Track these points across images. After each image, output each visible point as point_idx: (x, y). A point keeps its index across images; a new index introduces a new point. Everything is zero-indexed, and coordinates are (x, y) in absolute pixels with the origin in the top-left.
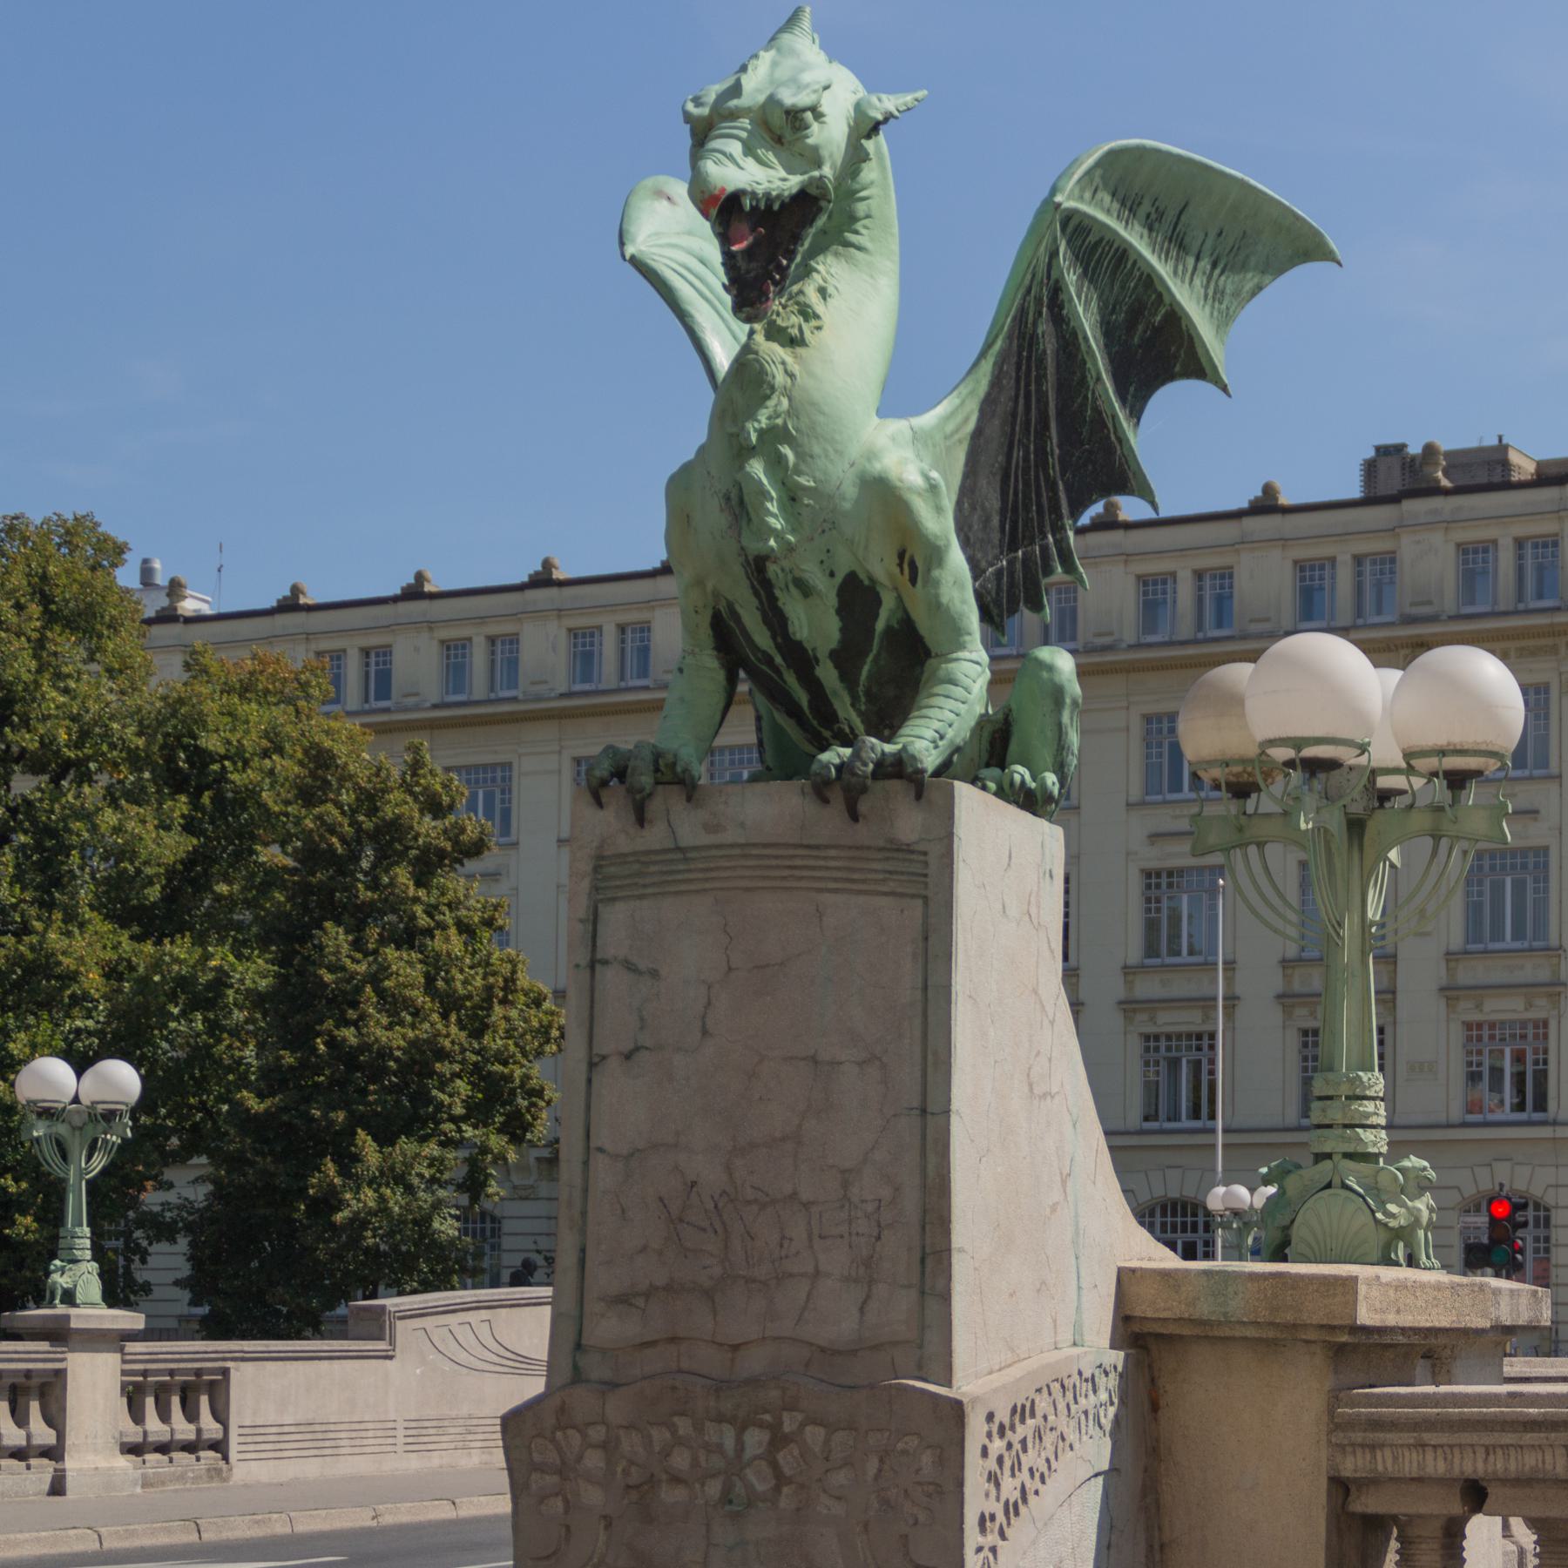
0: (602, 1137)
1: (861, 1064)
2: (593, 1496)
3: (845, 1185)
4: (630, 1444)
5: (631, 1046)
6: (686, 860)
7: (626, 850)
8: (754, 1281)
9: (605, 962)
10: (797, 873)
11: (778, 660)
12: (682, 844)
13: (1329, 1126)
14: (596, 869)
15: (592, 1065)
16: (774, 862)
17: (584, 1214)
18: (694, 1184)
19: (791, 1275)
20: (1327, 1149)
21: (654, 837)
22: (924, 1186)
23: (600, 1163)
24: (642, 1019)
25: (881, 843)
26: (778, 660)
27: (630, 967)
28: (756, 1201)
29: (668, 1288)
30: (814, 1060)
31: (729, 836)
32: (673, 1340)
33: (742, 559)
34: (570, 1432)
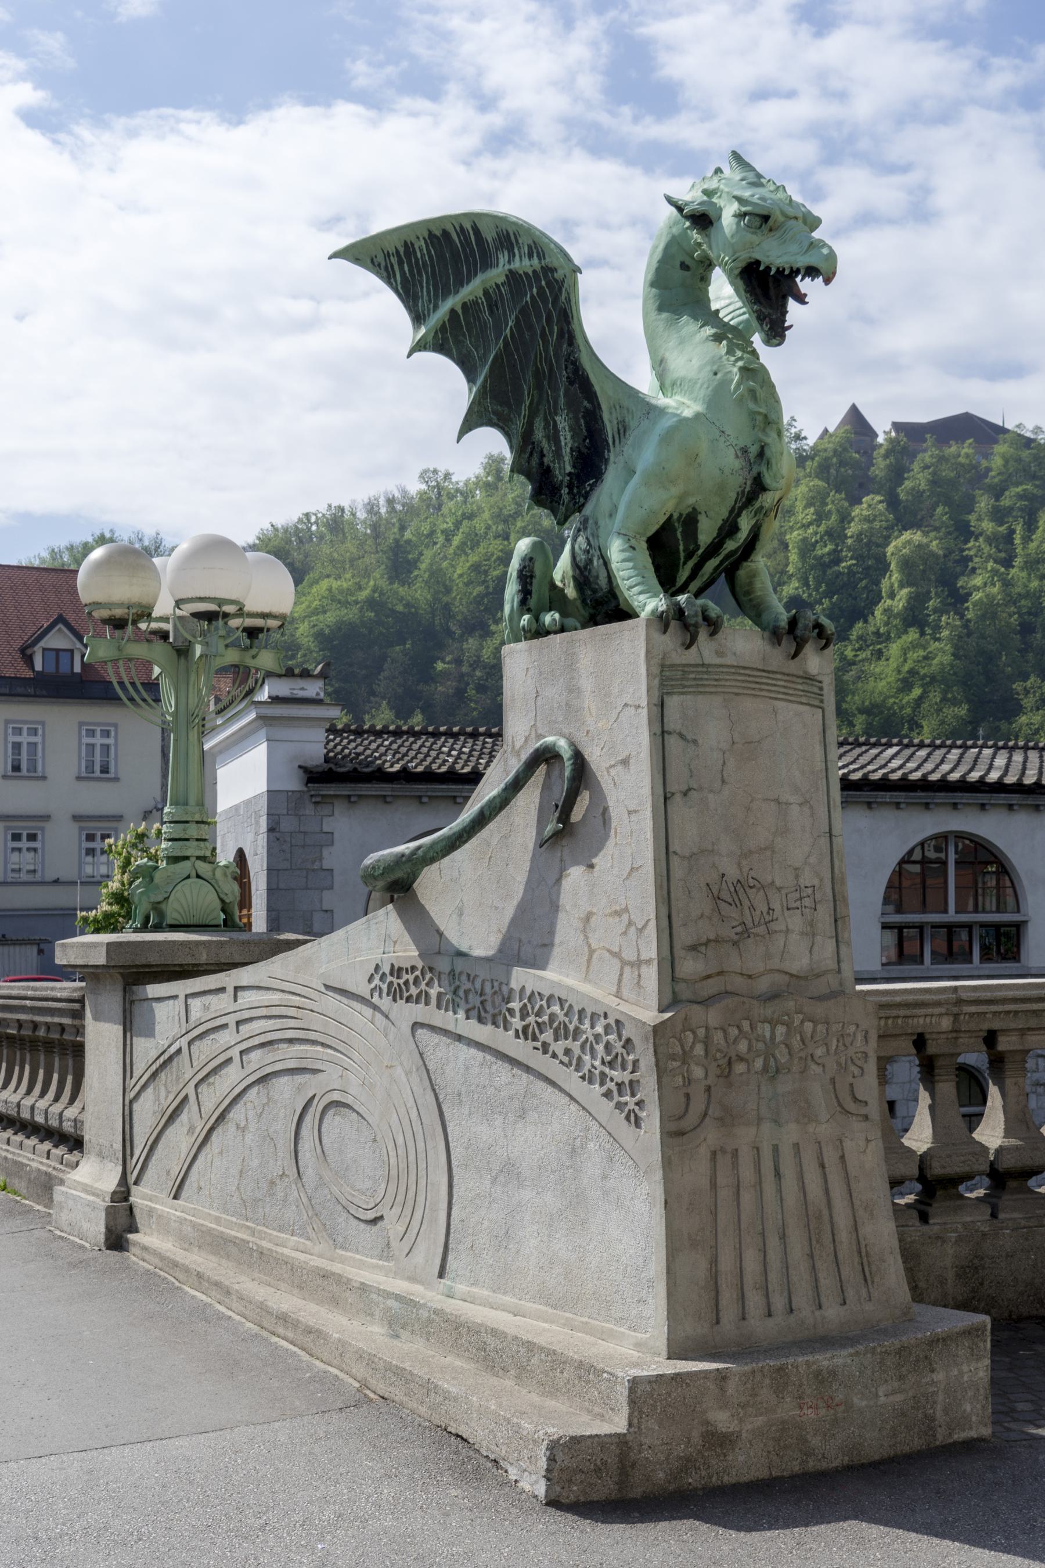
0: (674, 846)
1: (801, 805)
2: (698, 1072)
3: (797, 877)
4: (718, 1037)
5: (686, 788)
6: (707, 673)
7: (678, 662)
8: (758, 935)
9: (669, 733)
10: (763, 687)
11: (700, 552)
12: (706, 662)
13: (187, 840)
14: (662, 671)
15: (666, 799)
16: (751, 679)
17: (669, 893)
18: (723, 875)
19: (776, 932)
20: (188, 854)
21: (691, 656)
22: (833, 878)
23: (675, 861)
24: (691, 771)
25: (801, 673)
26: (700, 552)
27: (681, 735)
28: (754, 886)
29: (716, 941)
30: (778, 801)
31: (729, 660)
32: (720, 973)
33: (740, 490)
34: (688, 1033)
